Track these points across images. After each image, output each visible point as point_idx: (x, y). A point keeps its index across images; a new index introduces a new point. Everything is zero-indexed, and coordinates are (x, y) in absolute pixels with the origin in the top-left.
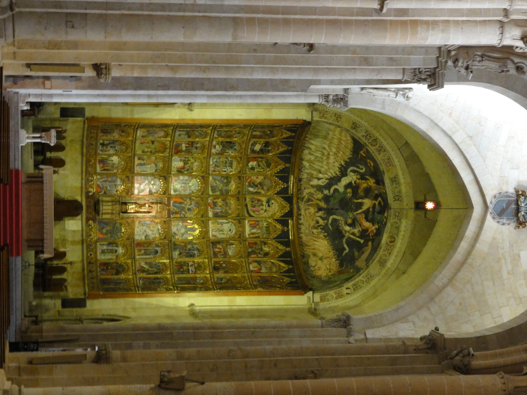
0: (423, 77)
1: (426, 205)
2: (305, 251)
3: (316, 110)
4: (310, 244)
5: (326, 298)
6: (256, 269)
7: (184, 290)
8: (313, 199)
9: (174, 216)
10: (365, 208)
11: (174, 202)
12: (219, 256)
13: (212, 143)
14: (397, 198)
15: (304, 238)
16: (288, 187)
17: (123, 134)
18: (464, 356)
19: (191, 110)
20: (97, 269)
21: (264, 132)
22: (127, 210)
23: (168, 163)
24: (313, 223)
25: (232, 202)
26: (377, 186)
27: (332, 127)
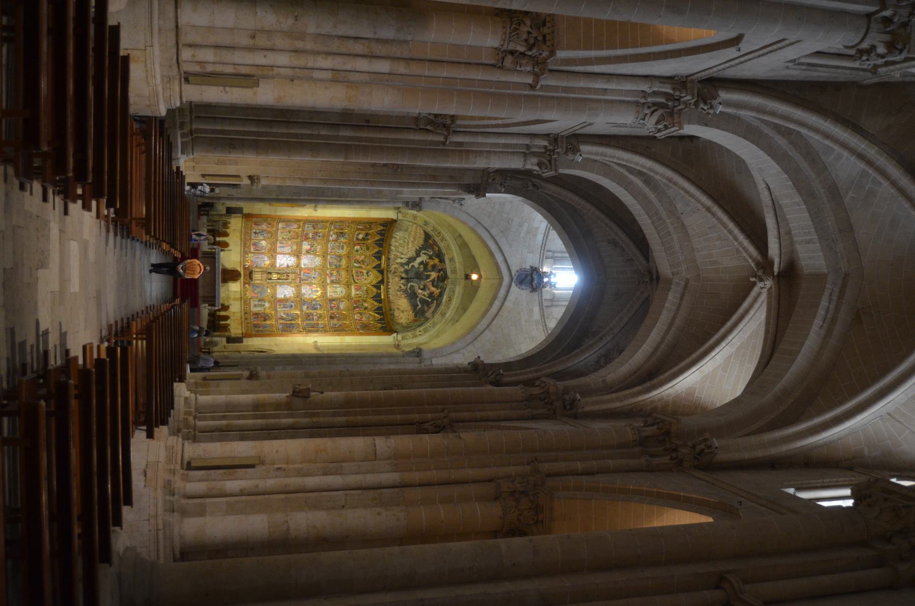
0: (472, 189)
3: (400, 212)
7: (310, 331)
9: (304, 282)
10: (432, 278)
11: (304, 273)
14: (453, 272)
15: (391, 298)
16: (380, 264)
17: (270, 226)
18: (496, 375)
19: (316, 211)
20: (251, 318)
21: (365, 226)
24: (397, 288)
25: (343, 273)
27: (411, 224)
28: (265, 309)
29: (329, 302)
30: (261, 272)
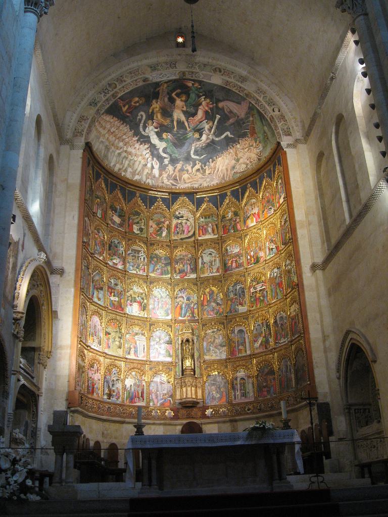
2: (229, 177)
4: (222, 175)
6: (254, 219)
8: (173, 175)
10: (183, 118)
11: (180, 315)
12: (241, 261)
13: (109, 264)
16: (161, 198)
22: (192, 369)
24: (199, 175)
25: (179, 253)
26: (160, 97)
28: (249, 377)
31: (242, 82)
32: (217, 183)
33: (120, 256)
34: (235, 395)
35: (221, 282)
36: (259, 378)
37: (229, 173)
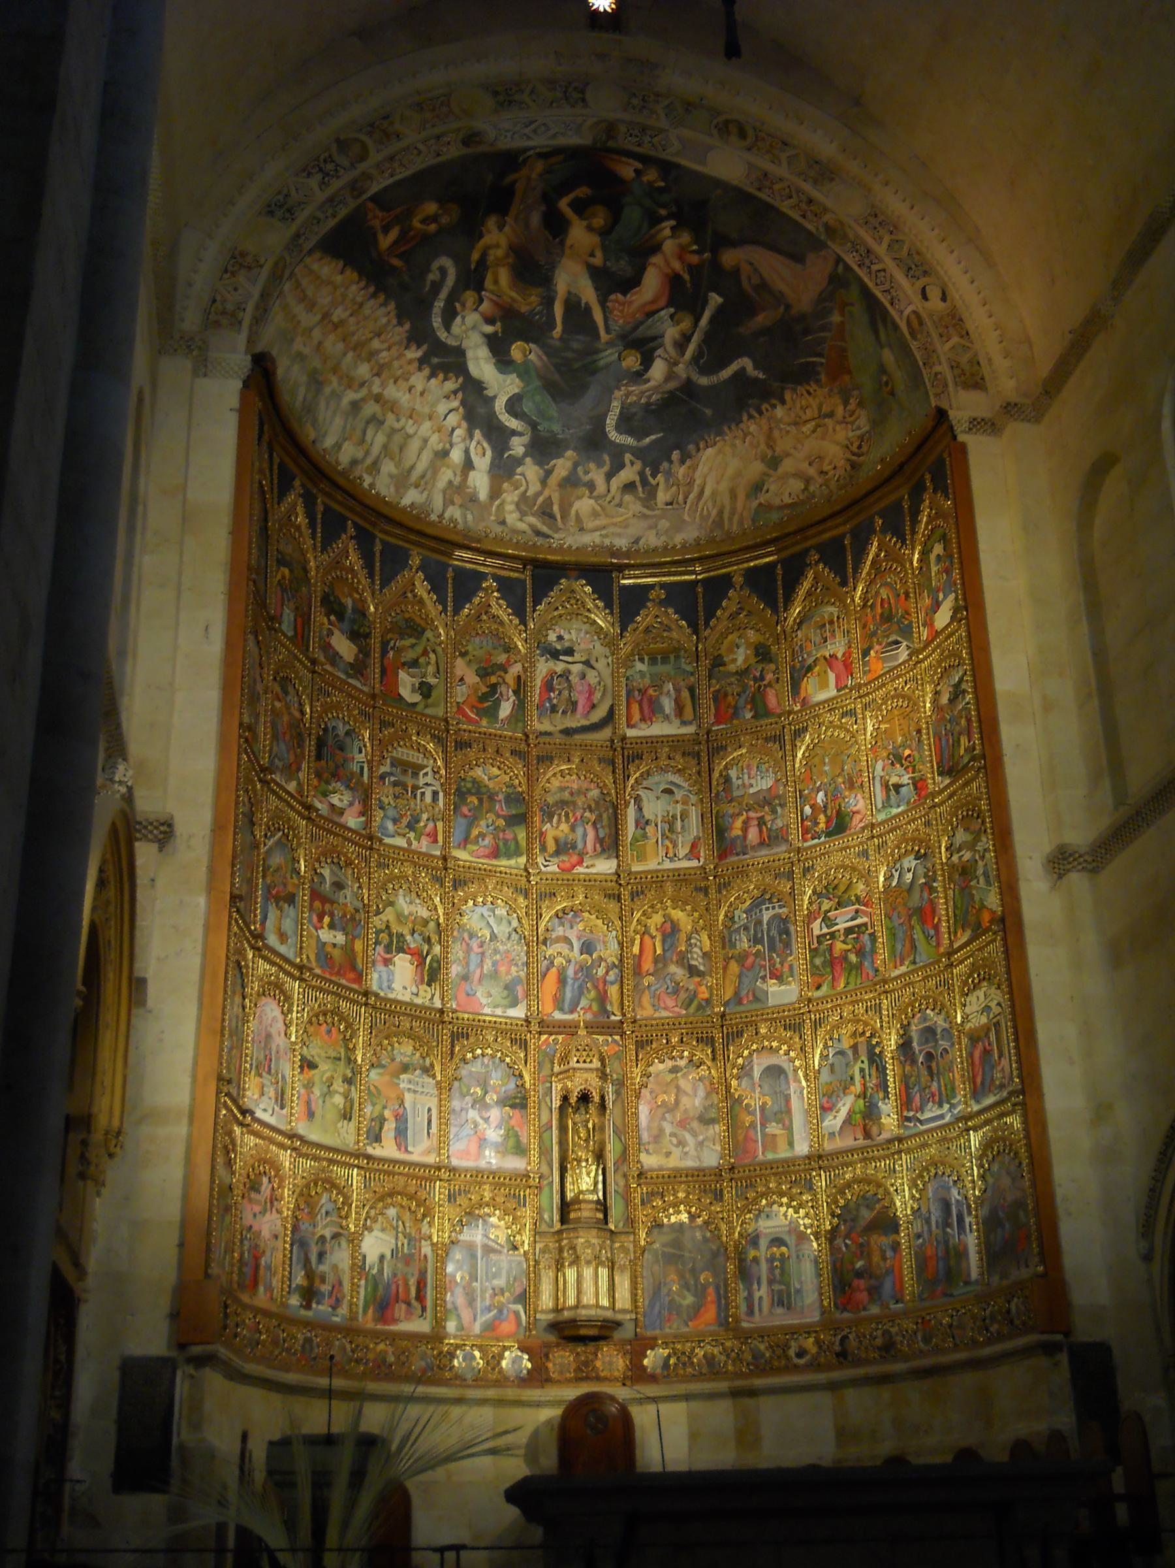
1: (601, 9)
2: (741, 522)
4: (714, 512)
5: (967, 368)
6: (832, 677)
8: (541, 499)
13: (317, 810)
15: (689, 534)
16: (496, 578)
20: (877, 1319)
23: (399, 1014)
24: (633, 505)
25: (556, 783)
28: (802, 1237)
29: (735, 858)
30: (559, 1266)
31: (816, 182)
32: (697, 541)
33: (352, 783)
34: (749, 1299)
35: (706, 894)
36: (839, 1241)
37: (739, 505)
